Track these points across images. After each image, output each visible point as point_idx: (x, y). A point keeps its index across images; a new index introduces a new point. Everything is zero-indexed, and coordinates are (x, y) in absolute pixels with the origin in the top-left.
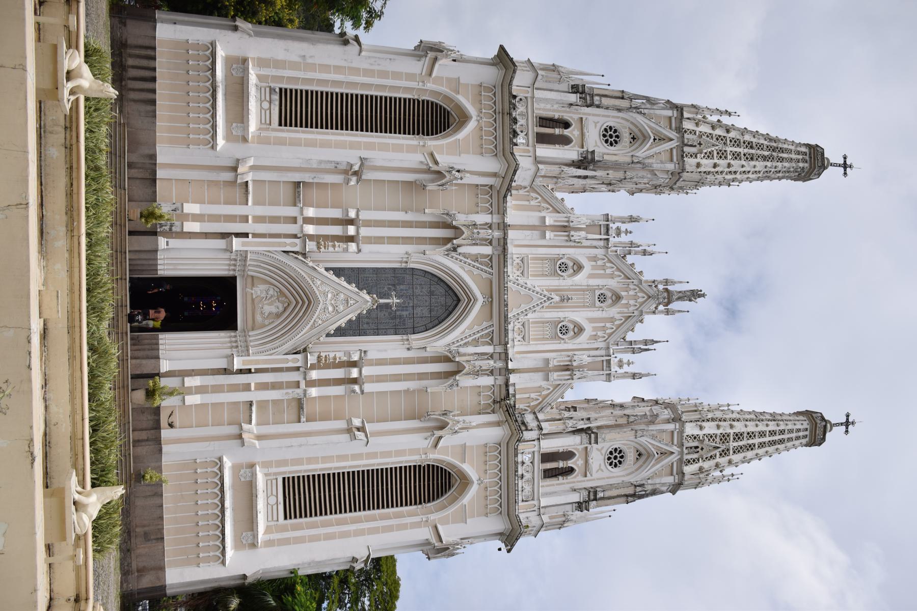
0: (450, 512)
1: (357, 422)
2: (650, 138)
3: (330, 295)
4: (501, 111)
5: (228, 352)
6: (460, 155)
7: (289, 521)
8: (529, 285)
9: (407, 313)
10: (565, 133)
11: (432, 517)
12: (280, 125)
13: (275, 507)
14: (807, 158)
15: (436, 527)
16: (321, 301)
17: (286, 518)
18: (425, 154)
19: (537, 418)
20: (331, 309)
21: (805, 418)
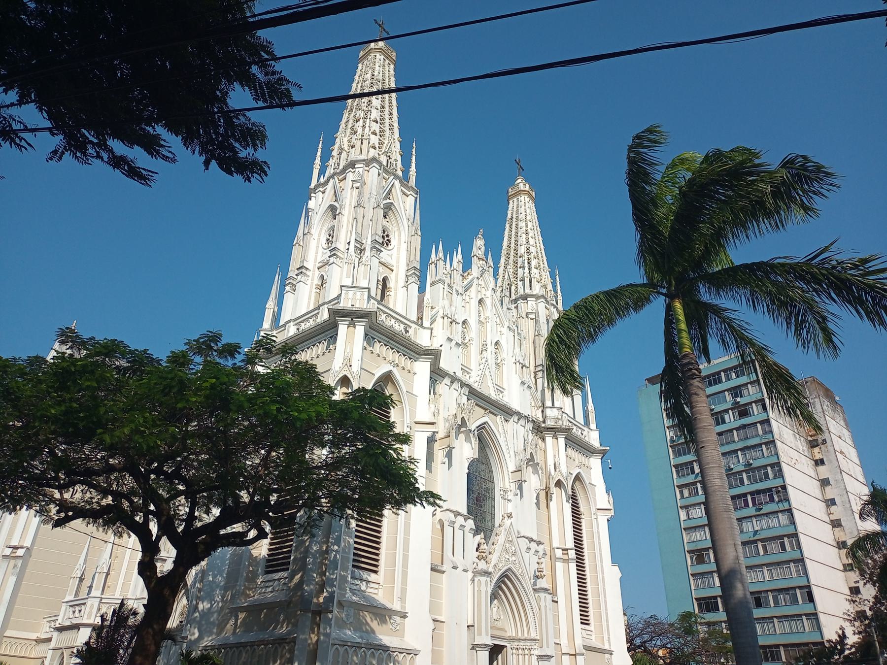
0: (591, 496)
1: (559, 553)
2: (392, 203)
3: (507, 557)
4: (388, 340)
5: (534, 658)
6: (417, 396)
7: (592, 622)
8: (480, 372)
9: (483, 484)
10: (381, 280)
11: (593, 510)
12: (376, 572)
13: (587, 632)
14: (387, 61)
15: (598, 509)
16: (510, 565)
17: (588, 624)
18: (416, 430)
19: (551, 408)
20: (514, 558)
21: (523, 196)
